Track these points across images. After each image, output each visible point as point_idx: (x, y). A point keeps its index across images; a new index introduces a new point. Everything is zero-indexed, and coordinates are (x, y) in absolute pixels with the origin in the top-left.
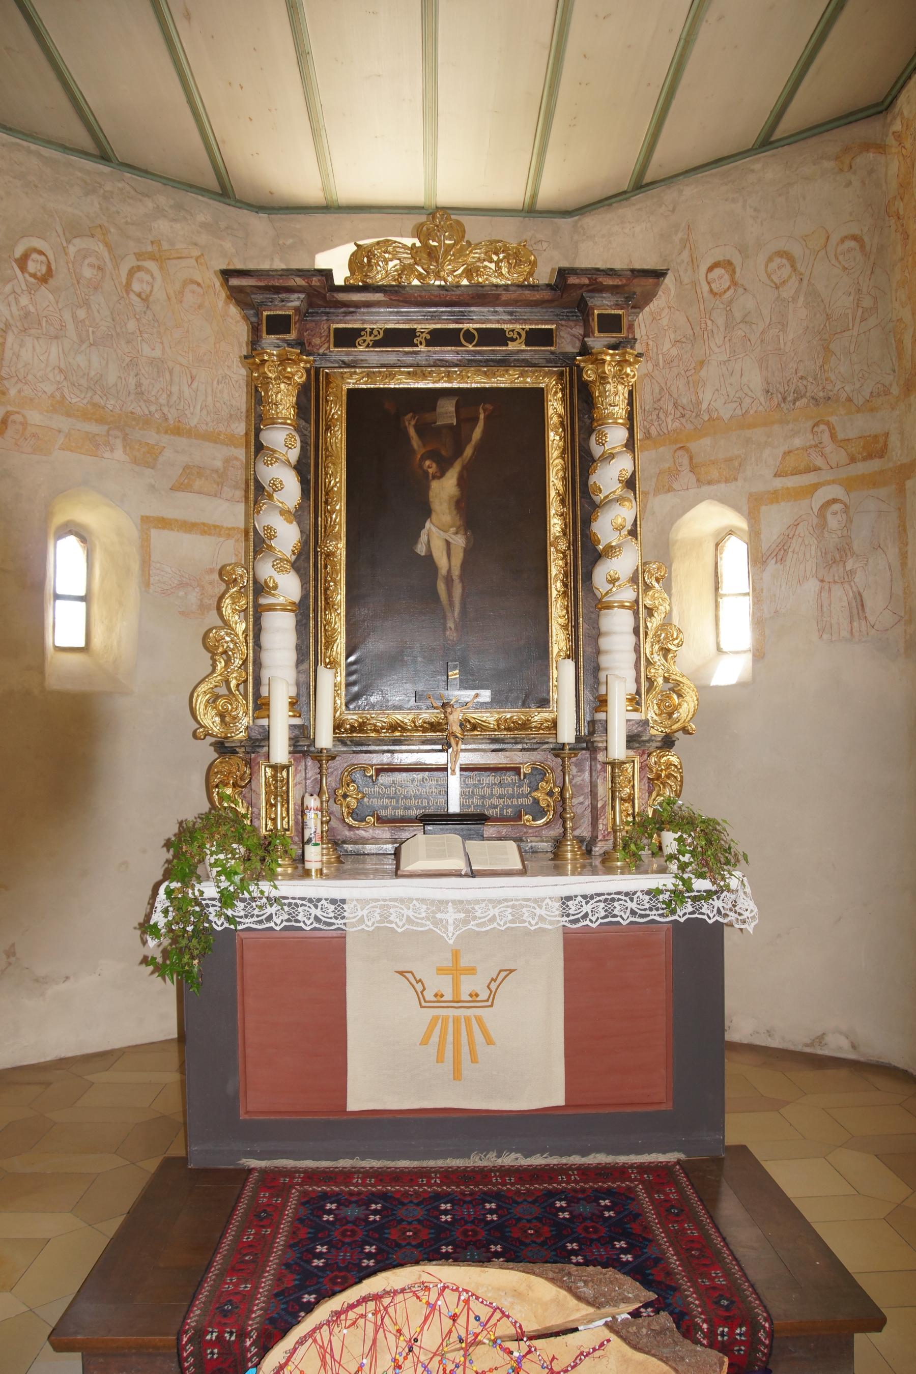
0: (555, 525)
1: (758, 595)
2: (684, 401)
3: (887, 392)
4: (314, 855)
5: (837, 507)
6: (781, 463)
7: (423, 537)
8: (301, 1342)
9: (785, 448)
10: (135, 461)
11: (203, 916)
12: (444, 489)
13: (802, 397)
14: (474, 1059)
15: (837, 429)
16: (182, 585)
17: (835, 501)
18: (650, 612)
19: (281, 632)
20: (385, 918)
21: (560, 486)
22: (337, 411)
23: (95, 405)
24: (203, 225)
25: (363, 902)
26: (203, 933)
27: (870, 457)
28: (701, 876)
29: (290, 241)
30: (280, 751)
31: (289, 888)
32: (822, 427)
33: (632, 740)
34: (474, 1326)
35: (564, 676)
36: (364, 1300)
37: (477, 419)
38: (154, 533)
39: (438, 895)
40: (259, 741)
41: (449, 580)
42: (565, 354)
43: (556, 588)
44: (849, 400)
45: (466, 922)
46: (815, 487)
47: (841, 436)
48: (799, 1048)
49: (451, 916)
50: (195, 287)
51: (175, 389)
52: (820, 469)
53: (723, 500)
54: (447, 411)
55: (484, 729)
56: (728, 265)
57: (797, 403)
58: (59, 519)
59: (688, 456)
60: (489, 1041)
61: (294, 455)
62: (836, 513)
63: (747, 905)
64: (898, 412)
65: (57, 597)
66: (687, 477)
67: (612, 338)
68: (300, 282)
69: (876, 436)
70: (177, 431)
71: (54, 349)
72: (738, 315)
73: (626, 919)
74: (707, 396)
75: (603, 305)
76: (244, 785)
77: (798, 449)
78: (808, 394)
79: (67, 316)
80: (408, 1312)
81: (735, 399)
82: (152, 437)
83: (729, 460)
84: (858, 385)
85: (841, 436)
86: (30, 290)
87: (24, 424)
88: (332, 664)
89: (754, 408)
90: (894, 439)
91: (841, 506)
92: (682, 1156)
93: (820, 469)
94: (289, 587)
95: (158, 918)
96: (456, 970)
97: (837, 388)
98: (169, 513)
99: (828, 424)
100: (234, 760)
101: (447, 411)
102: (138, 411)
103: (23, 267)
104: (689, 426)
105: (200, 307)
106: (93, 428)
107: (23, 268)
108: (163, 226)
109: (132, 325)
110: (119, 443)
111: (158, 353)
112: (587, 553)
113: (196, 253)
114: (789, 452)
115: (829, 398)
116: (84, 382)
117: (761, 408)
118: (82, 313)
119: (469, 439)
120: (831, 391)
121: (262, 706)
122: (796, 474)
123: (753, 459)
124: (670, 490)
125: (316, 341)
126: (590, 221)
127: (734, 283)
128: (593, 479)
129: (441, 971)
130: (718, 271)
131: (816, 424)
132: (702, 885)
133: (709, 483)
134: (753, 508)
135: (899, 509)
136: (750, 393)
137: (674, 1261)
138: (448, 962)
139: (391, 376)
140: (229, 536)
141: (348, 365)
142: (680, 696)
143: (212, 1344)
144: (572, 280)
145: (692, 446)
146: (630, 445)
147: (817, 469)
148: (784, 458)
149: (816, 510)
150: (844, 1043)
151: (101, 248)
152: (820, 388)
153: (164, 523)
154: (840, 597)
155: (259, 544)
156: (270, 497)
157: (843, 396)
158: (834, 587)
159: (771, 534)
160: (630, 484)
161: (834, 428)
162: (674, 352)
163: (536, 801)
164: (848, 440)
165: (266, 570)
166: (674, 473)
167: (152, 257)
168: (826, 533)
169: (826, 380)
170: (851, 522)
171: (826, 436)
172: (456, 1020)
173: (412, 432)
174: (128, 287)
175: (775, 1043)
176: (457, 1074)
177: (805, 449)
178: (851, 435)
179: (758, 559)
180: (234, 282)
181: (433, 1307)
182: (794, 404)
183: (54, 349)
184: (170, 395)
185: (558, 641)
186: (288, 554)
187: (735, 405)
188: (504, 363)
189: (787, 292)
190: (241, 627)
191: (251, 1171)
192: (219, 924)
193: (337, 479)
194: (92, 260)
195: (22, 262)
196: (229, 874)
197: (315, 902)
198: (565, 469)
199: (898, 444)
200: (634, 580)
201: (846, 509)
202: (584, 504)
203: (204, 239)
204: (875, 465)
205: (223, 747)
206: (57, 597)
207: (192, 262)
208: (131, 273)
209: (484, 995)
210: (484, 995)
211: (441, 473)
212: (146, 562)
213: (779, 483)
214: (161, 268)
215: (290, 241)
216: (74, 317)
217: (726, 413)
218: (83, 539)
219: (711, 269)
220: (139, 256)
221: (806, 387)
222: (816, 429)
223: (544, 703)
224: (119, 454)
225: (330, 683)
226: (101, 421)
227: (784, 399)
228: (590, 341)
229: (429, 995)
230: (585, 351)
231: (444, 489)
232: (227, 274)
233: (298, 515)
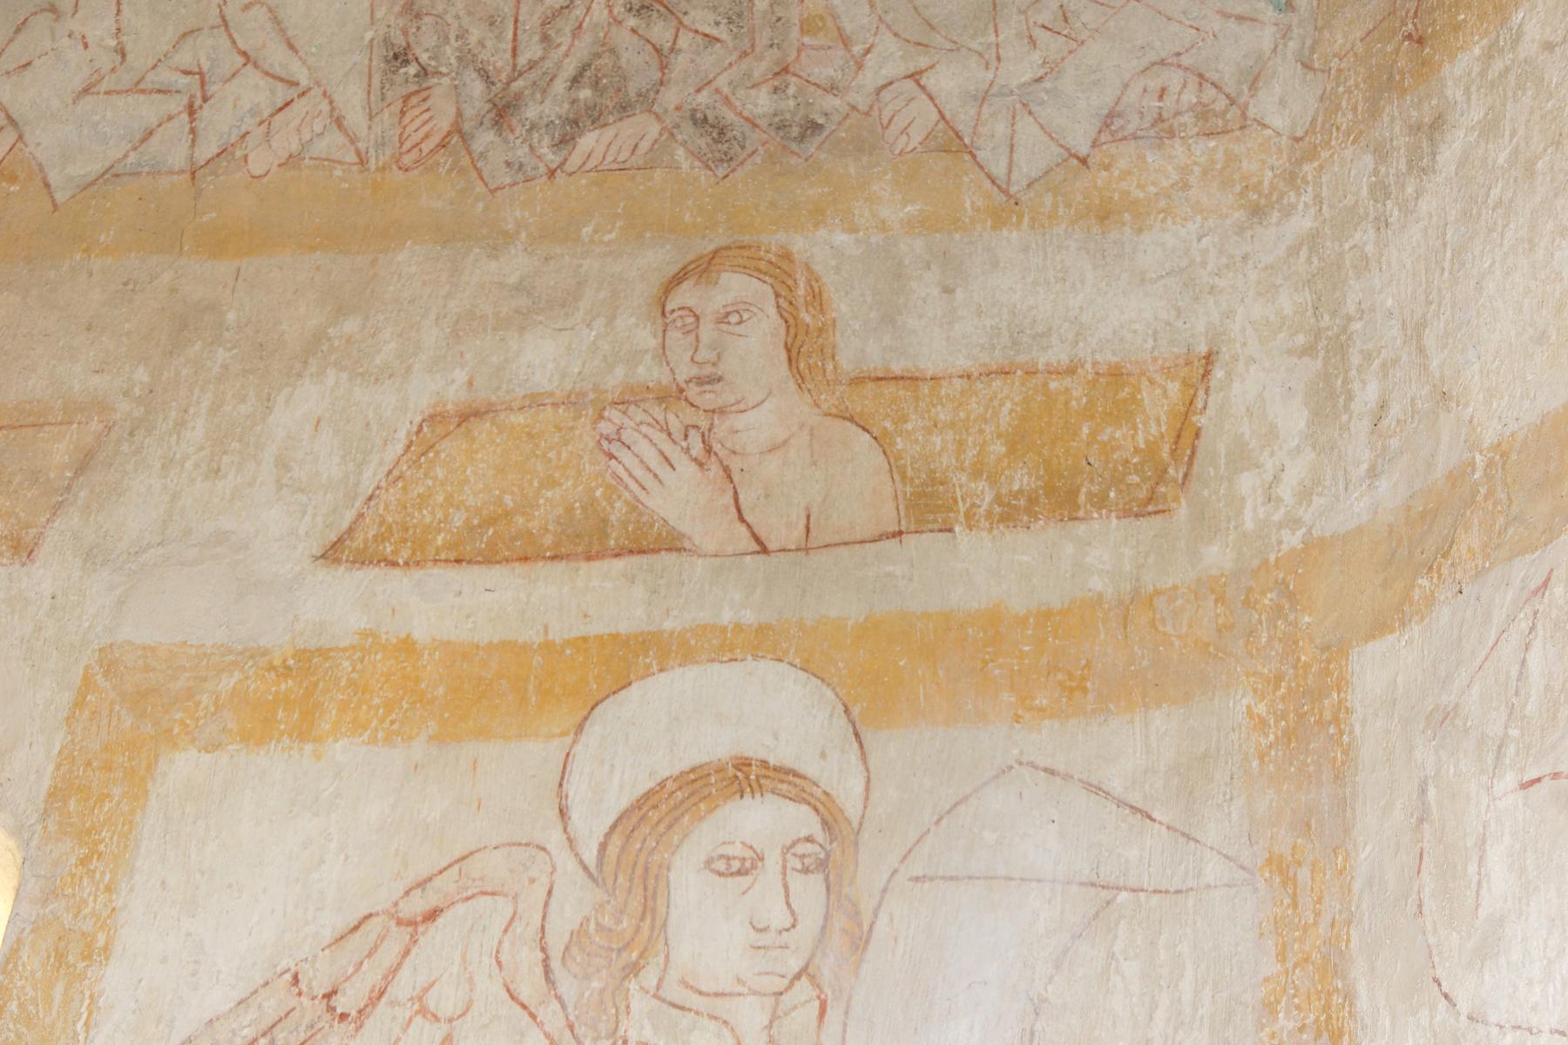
3: (1223, 115)
5: (756, 820)
6: (393, 476)
9: (452, 388)
13: (624, 109)
15: (841, 306)
17: (746, 776)
27: (1059, 500)
32: (735, 286)
44: (952, 143)
46: (621, 661)
52: (672, 543)
57: (589, 141)
62: (743, 867)
64: (1302, 223)
69: (1116, 374)
77: (535, 401)
78: (670, 97)
81: (165, 76)
84: (1020, 69)
85: (858, 347)
89: (285, 142)
90: (1261, 394)
91: (801, 820)
93: (672, 543)
97: (870, 78)
99: (780, 271)
114: (469, 415)
115: (815, 127)
117: (331, 143)
120: (832, 88)
122: (489, 558)
123: (197, 432)
131: (703, 269)
135: (1281, 868)
136: (276, 56)
147: (651, 541)
148: (422, 445)
149: (591, 825)
152: (760, 69)
157: (922, 116)
161: (817, 298)
164: (910, 380)
168: (639, 1003)
169: (807, 27)
170: (860, 942)
171: (756, 347)
178: (940, 340)
182: (565, 142)
187: (148, 110)
199: (1293, 419)
204: (1098, 555)
213: (342, 605)
221: (663, 57)
222: (686, 295)
227: (502, 112)
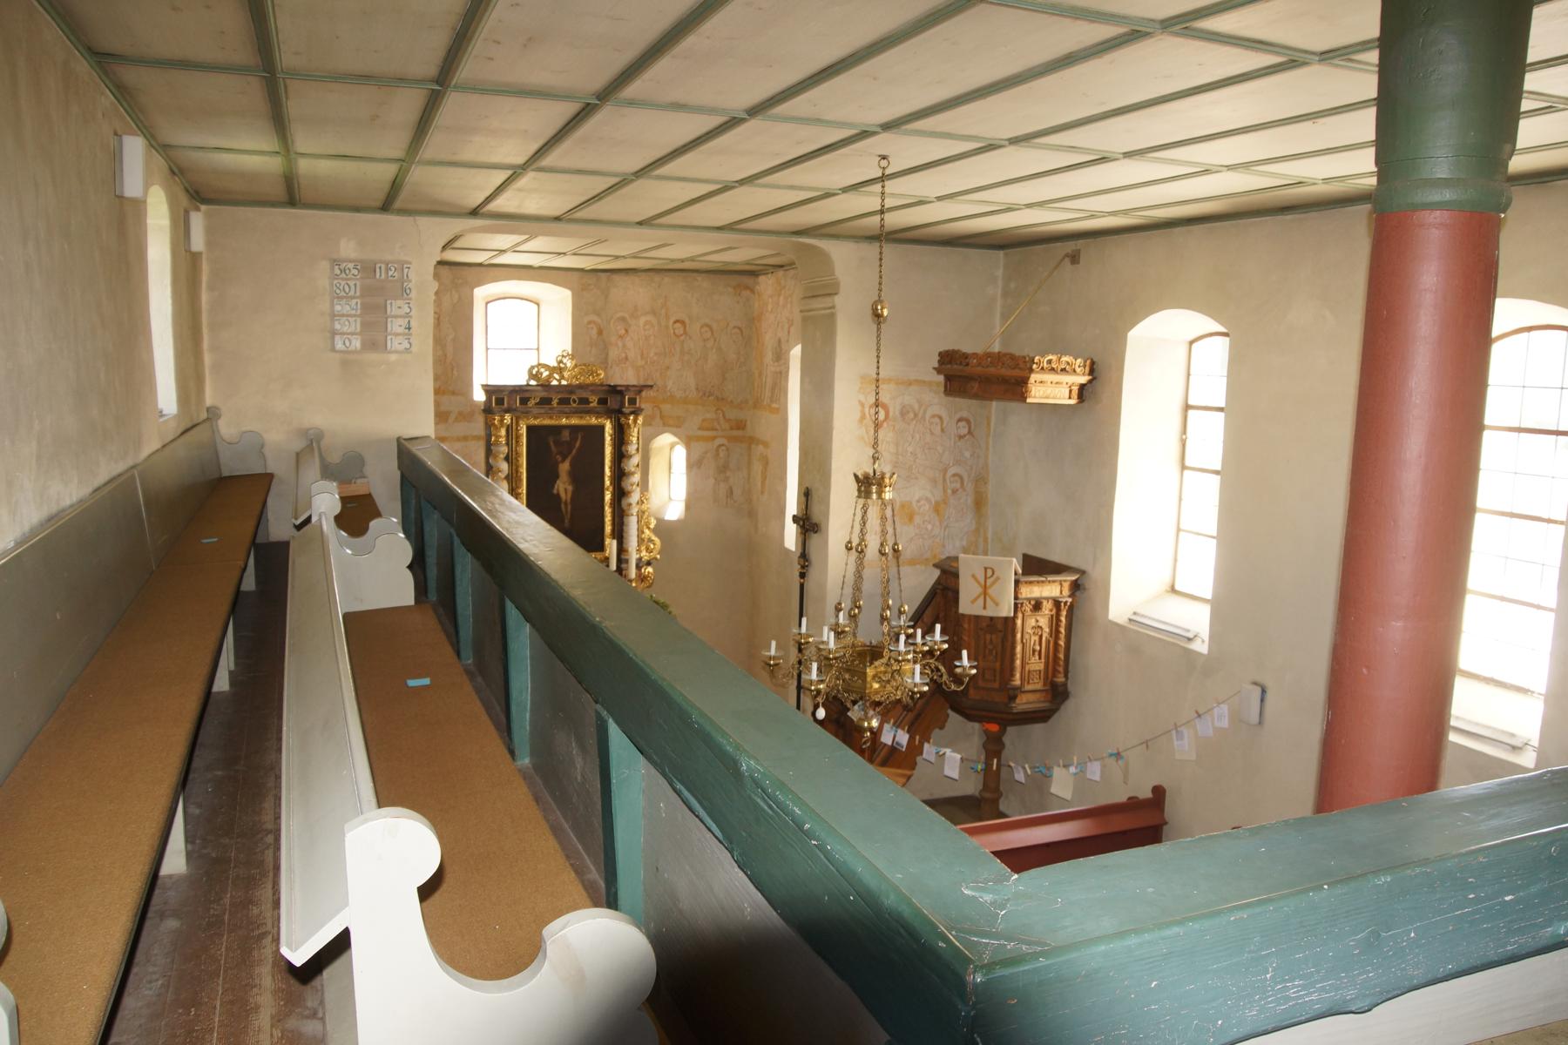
0: (607, 483)
12: (564, 467)
35: (611, 545)
46: (714, 438)
54: (566, 435)
56: (683, 323)
74: (670, 384)
101: (566, 435)
112: (620, 494)
126: (616, 277)
127: (685, 333)
134: (688, 442)
188: (590, 412)
189: (710, 344)
202: (620, 474)
211: (563, 460)
217: (679, 394)
231: (564, 467)
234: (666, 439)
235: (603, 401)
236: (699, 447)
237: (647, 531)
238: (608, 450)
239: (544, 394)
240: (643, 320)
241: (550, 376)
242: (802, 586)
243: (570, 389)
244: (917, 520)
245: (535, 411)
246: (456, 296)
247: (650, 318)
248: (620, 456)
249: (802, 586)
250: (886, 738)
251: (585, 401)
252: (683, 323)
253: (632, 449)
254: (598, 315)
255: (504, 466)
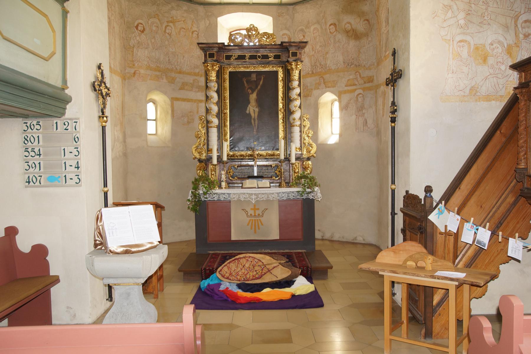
0: (281, 105)
1: (342, 119)
2: (322, 63)
3: (374, 65)
4: (224, 184)
5: (361, 95)
7: (248, 109)
8: (225, 266)
10: (169, 82)
11: (200, 198)
12: (253, 97)
14: (259, 229)
16: (182, 116)
17: (360, 94)
18: (304, 126)
19: (214, 133)
20: (239, 197)
21: (282, 96)
22: (227, 76)
23: (158, 67)
24: (185, 11)
25: (234, 194)
26: (200, 201)
27: (369, 82)
28: (308, 188)
29: (210, 14)
30: (215, 161)
31: (217, 191)
33: (297, 159)
34: (255, 263)
35: (282, 143)
36: (235, 259)
37: (261, 79)
38: (175, 102)
39: (251, 192)
40: (209, 159)
41: (254, 119)
42: (283, 62)
43: (281, 121)
44: (364, 66)
45: (257, 198)
46: (356, 90)
47: (362, 76)
48: (350, 241)
49: (254, 197)
50: (183, 30)
51: (179, 60)
53: (332, 92)
54: (254, 76)
55: (263, 156)
56: (335, 25)
58: (148, 98)
59: (324, 80)
60: (262, 225)
61: (216, 89)
63: (319, 195)
65: (148, 120)
66: (323, 85)
67: (294, 58)
68: (217, 45)
70: (180, 72)
71: (146, 52)
72: (337, 40)
73: (292, 198)
74: (328, 62)
75: (292, 50)
76: (205, 169)
79: (149, 42)
80: (243, 261)
82: (173, 75)
83: (334, 81)
85: (362, 76)
86: (139, 35)
87: (140, 73)
88: (226, 140)
90: (375, 77)
92: (305, 251)
94: (215, 121)
95: (190, 198)
96: (255, 209)
98: (179, 96)
99: (359, 72)
100: (203, 164)
101: (254, 76)
102: (169, 67)
103: (137, 29)
104: (324, 71)
105: (185, 35)
106: (158, 73)
107: (137, 29)
108: (174, 12)
109: (167, 43)
110: (164, 77)
111: (174, 50)
112: (288, 112)
113: (183, 19)
116: (154, 60)
118: (153, 41)
119: (259, 84)
121: (209, 150)
124: (318, 89)
125: (221, 58)
126: (298, 7)
127: (336, 30)
128: (290, 94)
129: (251, 209)
130: (332, 26)
132: (309, 190)
133: (329, 87)
134: (340, 95)
137: (296, 261)
138: (253, 207)
139: (240, 68)
140: (195, 102)
141: (229, 65)
142: (312, 147)
143: (208, 270)
144: (284, 44)
145: (324, 77)
146: (299, 85)
147: (356, 85)
150: (361, 239)
151: (157, 21)
153: (177, 99)
154: (361, 120)
155: (208, 111)
156: (210, 100)
157: (363, 65)
158: (360, 117)
159: (344, 102)
160: (300, 95)
162: (320, 49)
163: (276, 173)
165: (210, 118)
166: (319, 84)
167: (171, 22)
171: (358, 76)
172: (255, 220)
173: (245, 82)
174: (165, 31)
175: (344, 240)
176: (255, 232)
177: (353, 79)
179: (343, 108)
180: (200, 46)
181: (248, 260)
183: (146, 52)
184: (178, 62)
185: (281, 134)
186: (215, 114)
188: (269, 63)
190: (203, 132)
191: (209, 254)
192: (203, 199)
193: (227, 94)
194: (155, 25)
195: (137, 27)
196: (206, 188)
197: (224, 194)
198: (283, 91)
200: (300, 119)
201: (363, 96)
202: (288, 100)
203: (185, 15)
204: (370, 84)
205: (200, 161)
206: (148, 120)
207: (182, 22)
208: (166, 27)
209: (261, 214)
210: (261, 214)
211: (252, 93)
212: (173, 111)
213: (346, 88)
214: (174, 25)
215: (210, 14)
216: (151, 42)
217: (333, 67)
218: (154, 103)
219: (330, 25)
220: (168, 22)
223: (278, 149)
224: (165, 80)
225: (226, 145)
226: (159, 71)
228: (289, 59)
229: (249, 214)
230: (288, 61)
231: (253, 97)
232: (199, 44)
233: (217, 104)
234: (328, 97)
235: (277, 57)
236: (346, 98)
237: (307, 138)
238: (281, 85)
239: (239, 53)
240: (312, 28)
241: (243, 41)
242: (393, 129)
243: (255, 48)
244: (491, 61)
245: (235, 63)
246: (208, 22)
247: (316, 26)
248: (288, 89)
249: (393, 129)
250: (467, 237)
251: (266, 57)
252: (335, 25)
253: (295, 83)
254: (288, 30)
255: (215, 96)
